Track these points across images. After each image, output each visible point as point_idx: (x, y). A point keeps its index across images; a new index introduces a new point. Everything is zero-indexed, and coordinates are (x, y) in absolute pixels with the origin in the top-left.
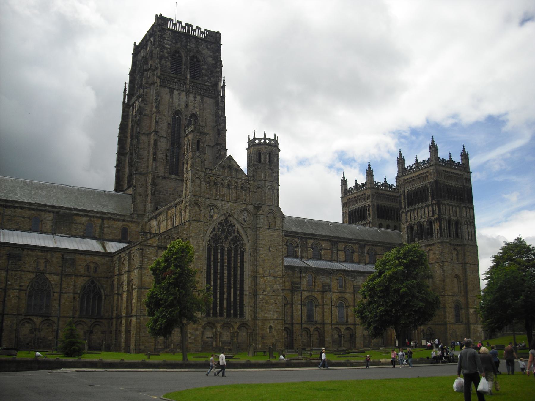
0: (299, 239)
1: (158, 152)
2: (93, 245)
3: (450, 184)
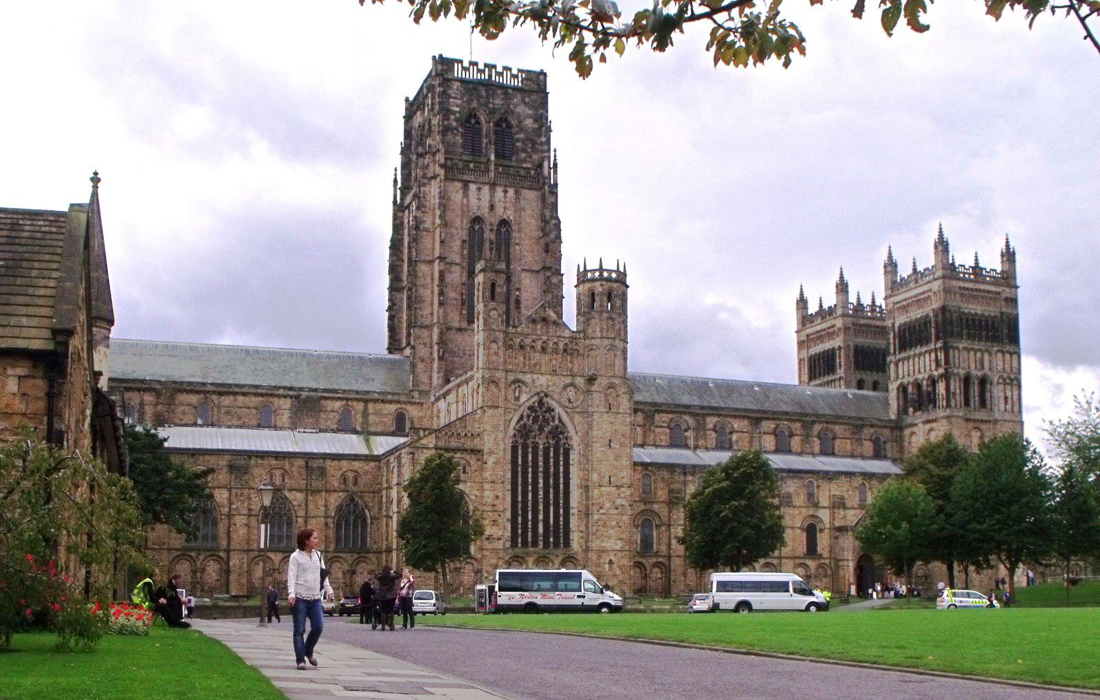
1: (445, 290)
2: (352, 444)
3: (973, 312)
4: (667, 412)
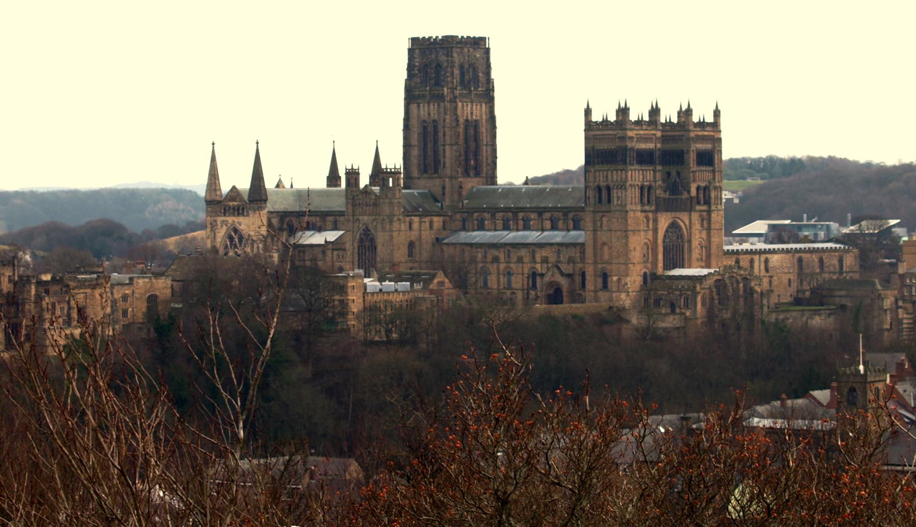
3: (602, 148)
4: (501, 212)
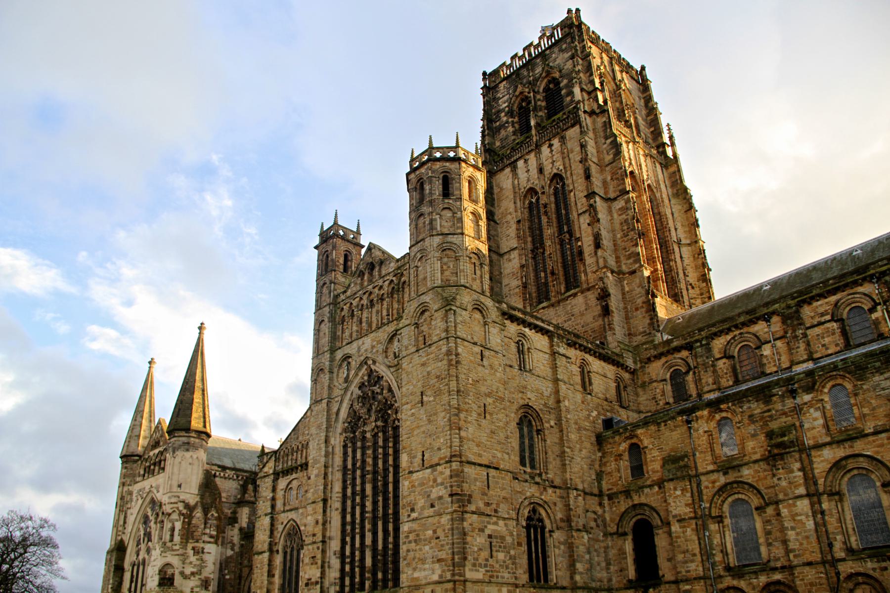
0: (871, 282)
4: (822, 296)
